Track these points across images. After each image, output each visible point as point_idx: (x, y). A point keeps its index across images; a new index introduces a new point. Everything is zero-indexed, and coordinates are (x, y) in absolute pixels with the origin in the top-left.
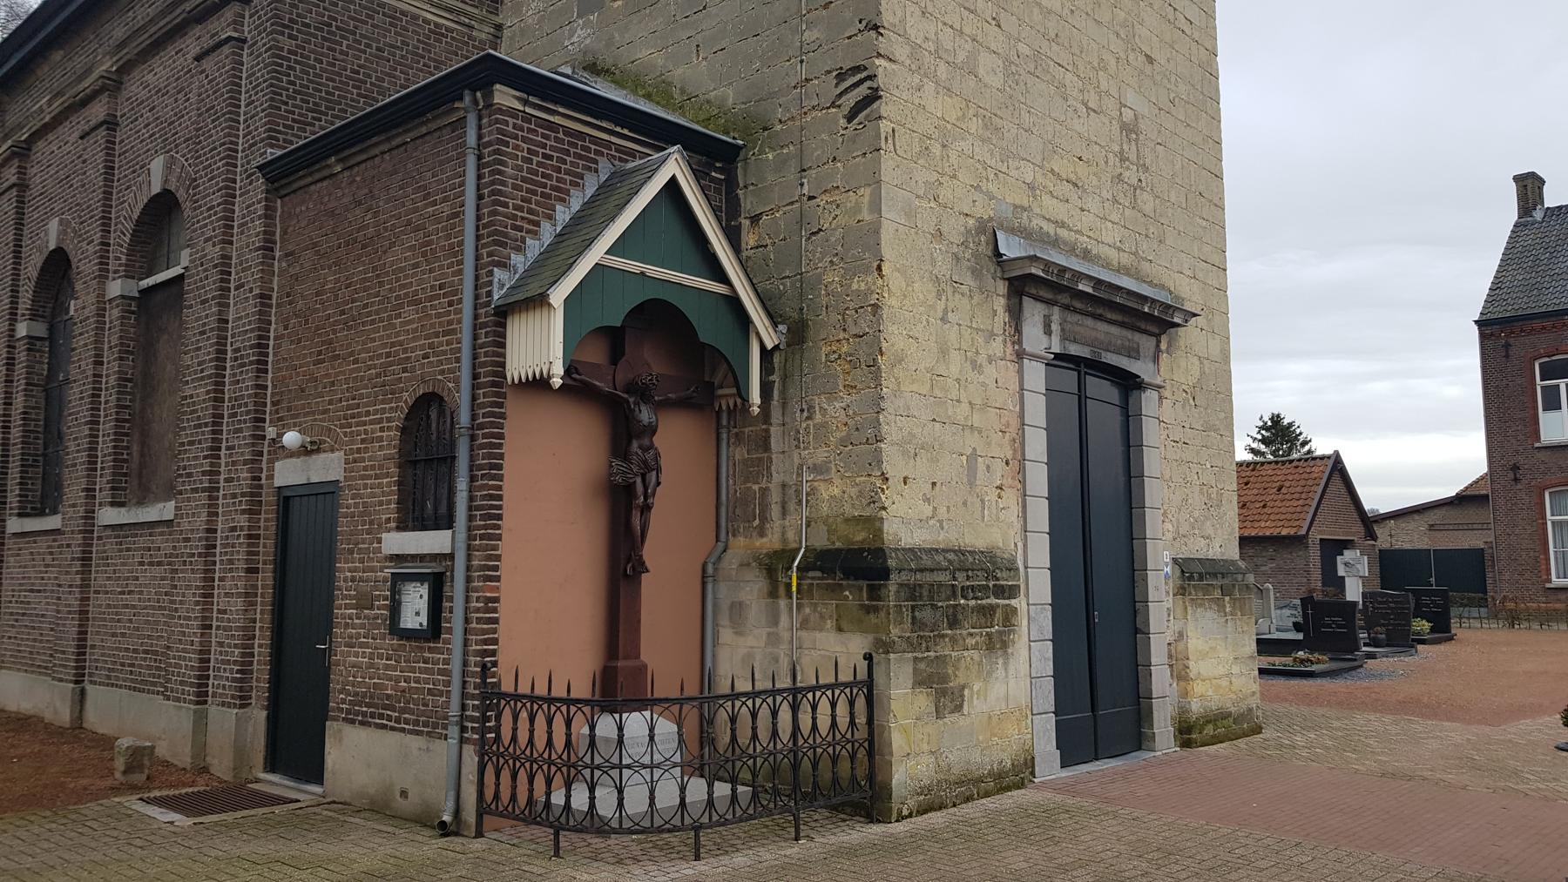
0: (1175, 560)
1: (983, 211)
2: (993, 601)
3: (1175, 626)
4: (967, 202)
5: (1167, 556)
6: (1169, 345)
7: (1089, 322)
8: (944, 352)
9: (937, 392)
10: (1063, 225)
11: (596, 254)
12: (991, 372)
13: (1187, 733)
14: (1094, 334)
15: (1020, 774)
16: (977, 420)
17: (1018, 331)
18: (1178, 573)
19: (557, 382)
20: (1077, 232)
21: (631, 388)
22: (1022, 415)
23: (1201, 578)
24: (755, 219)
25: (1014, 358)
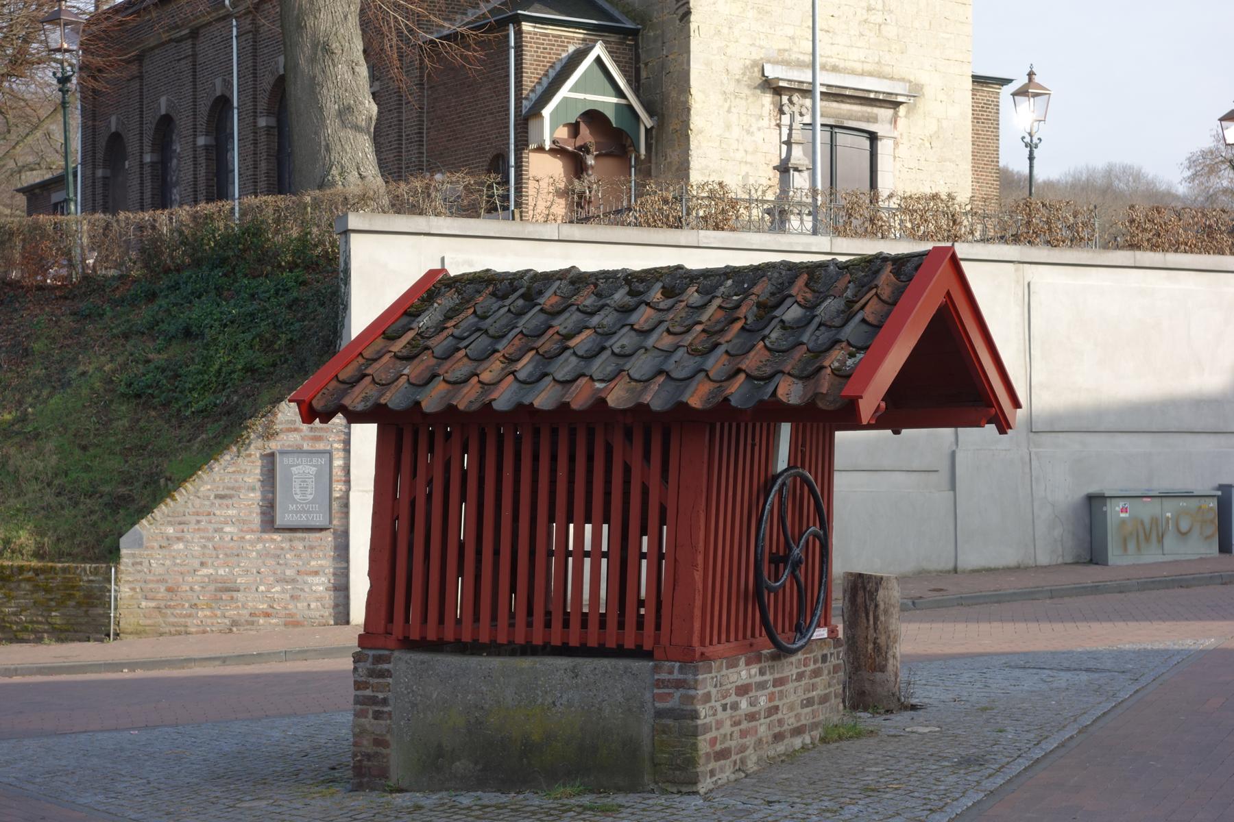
1: (757, 55)
4: (743, 53)
6: (908, 112)
8: (728, 127)
9: (724, 146)
11: (564, 92)
12: (759, 136)
16: (749, 158)
19: (547, 148)
21: (580, 148)
24: (646, 64)
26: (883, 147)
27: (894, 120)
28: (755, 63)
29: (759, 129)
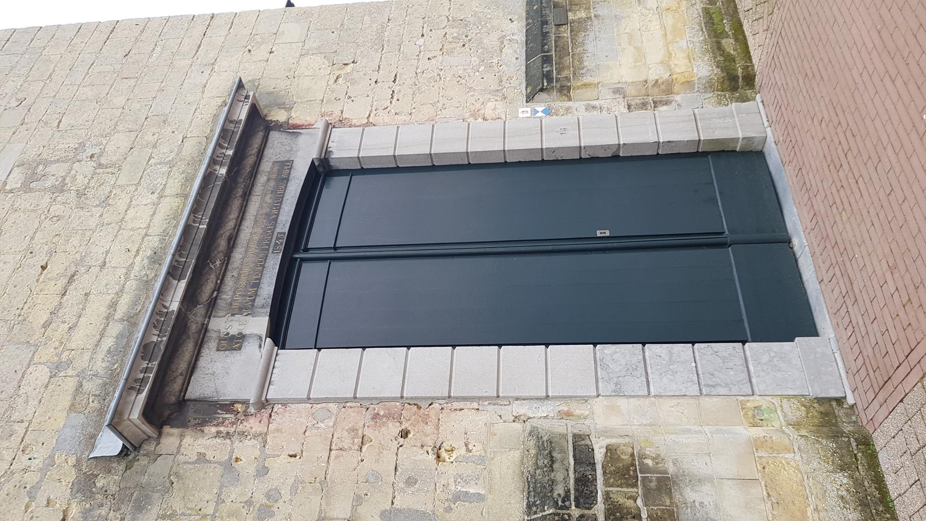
0: (530, 98)
2: (599, 508)
3: (606, 99)
5: (524, 111)
6: (281, 106)
7: (237, 255)
10: (113, 305)
13: (736, 81)
14: (253, 247)
15: (842, 433)
17: (228, 406)
18: (543, 95)
20: (127, 278)
22: (342, 402)
23: (547, 60)
25: (265, 413)
26: (344, 148)
27: (292, 129)
28: (85, 486)
29: (263, 471)
